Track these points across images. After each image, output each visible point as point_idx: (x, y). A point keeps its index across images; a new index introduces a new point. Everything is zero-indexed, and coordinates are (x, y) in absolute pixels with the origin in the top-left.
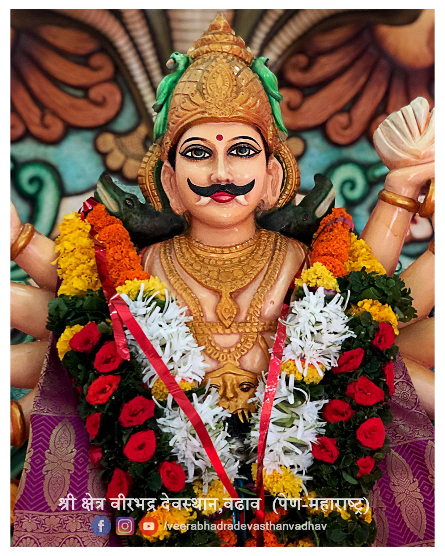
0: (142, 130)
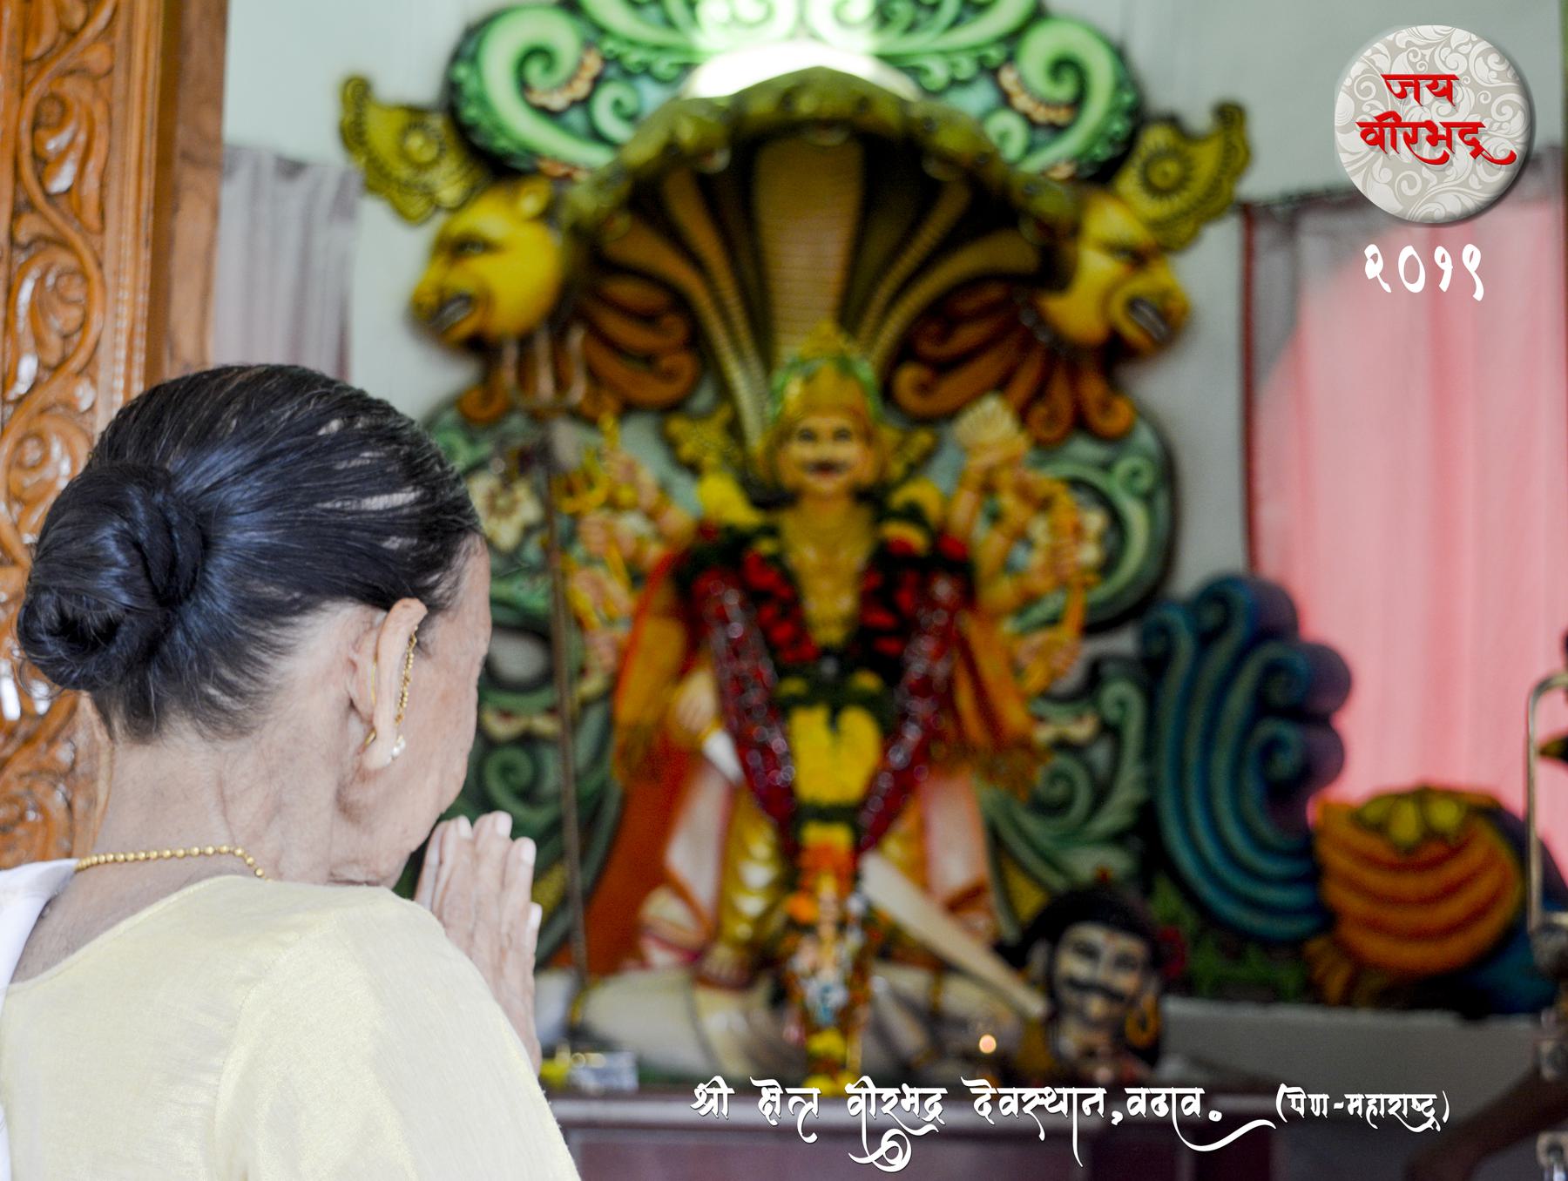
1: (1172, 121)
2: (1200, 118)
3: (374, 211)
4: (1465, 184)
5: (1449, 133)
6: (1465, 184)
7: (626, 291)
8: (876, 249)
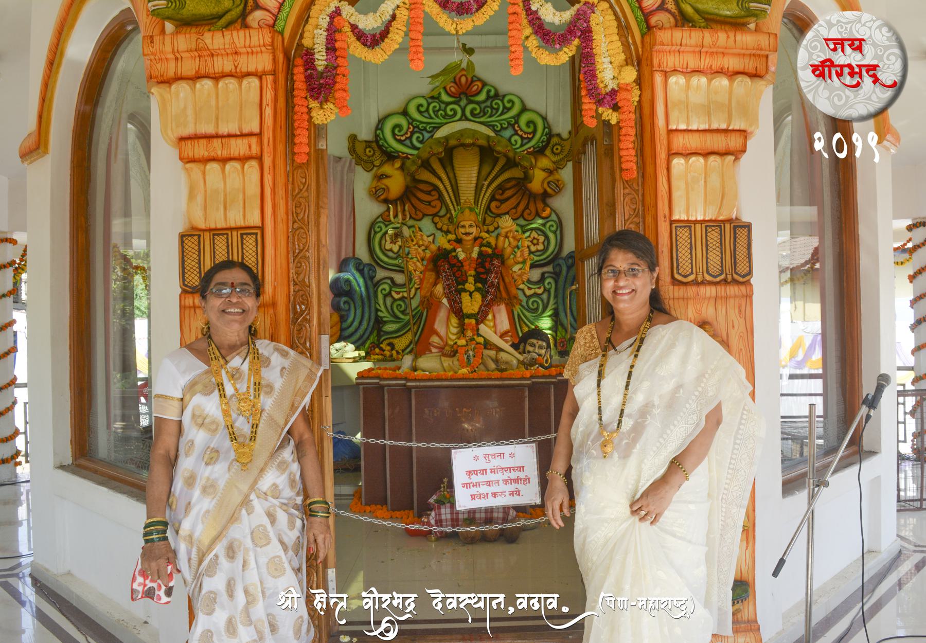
0: (448, 215)
1: (559, 135)
2: (565, 135)
3: (359, 169)
7: (422, 186)
8: (484, 173)
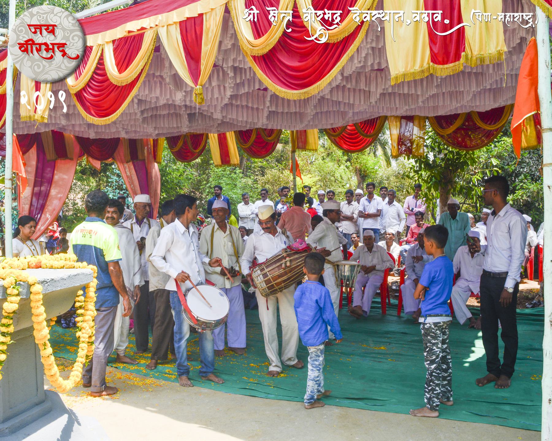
4: (60, 67)
5: (53, 47)
6: (60, 67)
